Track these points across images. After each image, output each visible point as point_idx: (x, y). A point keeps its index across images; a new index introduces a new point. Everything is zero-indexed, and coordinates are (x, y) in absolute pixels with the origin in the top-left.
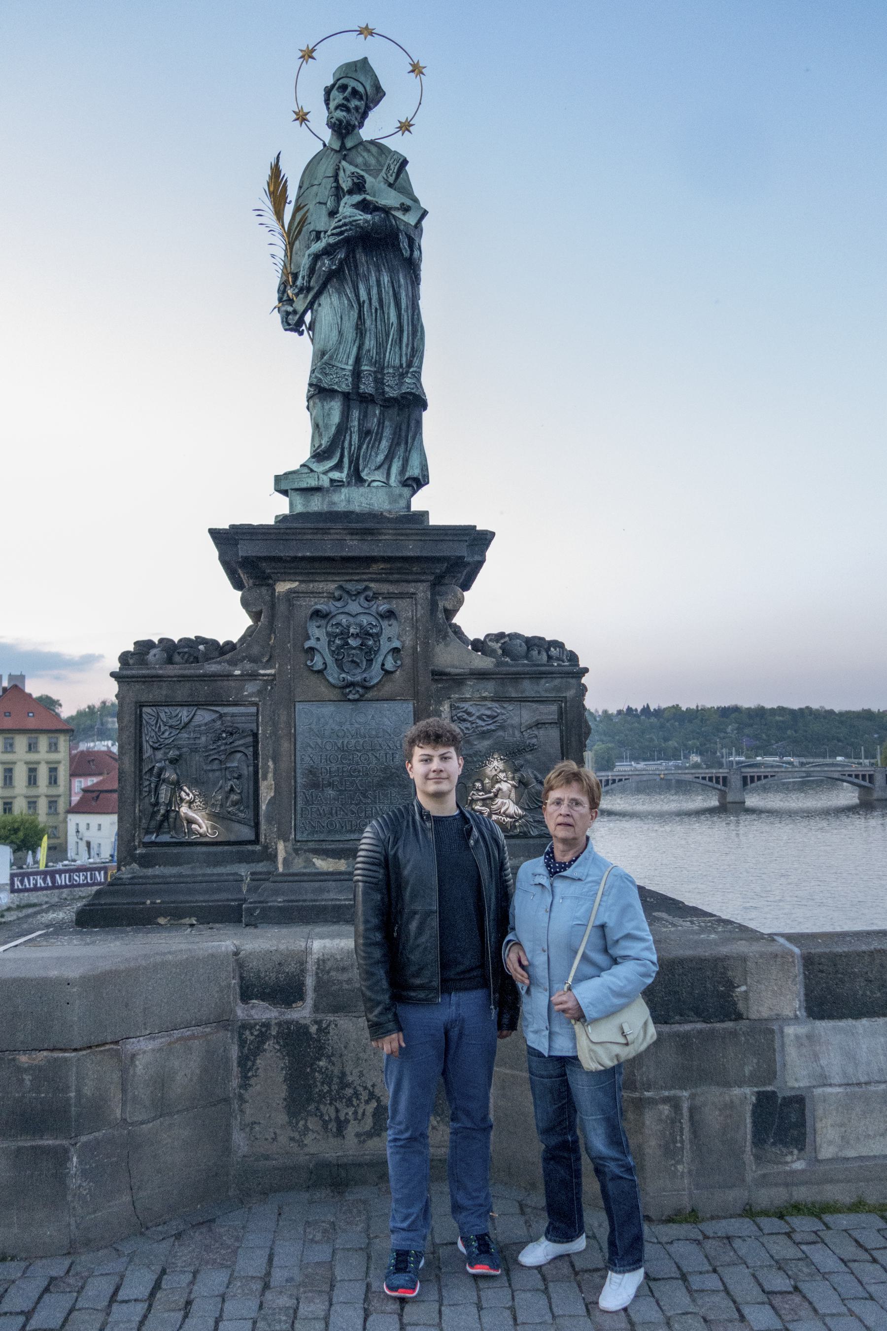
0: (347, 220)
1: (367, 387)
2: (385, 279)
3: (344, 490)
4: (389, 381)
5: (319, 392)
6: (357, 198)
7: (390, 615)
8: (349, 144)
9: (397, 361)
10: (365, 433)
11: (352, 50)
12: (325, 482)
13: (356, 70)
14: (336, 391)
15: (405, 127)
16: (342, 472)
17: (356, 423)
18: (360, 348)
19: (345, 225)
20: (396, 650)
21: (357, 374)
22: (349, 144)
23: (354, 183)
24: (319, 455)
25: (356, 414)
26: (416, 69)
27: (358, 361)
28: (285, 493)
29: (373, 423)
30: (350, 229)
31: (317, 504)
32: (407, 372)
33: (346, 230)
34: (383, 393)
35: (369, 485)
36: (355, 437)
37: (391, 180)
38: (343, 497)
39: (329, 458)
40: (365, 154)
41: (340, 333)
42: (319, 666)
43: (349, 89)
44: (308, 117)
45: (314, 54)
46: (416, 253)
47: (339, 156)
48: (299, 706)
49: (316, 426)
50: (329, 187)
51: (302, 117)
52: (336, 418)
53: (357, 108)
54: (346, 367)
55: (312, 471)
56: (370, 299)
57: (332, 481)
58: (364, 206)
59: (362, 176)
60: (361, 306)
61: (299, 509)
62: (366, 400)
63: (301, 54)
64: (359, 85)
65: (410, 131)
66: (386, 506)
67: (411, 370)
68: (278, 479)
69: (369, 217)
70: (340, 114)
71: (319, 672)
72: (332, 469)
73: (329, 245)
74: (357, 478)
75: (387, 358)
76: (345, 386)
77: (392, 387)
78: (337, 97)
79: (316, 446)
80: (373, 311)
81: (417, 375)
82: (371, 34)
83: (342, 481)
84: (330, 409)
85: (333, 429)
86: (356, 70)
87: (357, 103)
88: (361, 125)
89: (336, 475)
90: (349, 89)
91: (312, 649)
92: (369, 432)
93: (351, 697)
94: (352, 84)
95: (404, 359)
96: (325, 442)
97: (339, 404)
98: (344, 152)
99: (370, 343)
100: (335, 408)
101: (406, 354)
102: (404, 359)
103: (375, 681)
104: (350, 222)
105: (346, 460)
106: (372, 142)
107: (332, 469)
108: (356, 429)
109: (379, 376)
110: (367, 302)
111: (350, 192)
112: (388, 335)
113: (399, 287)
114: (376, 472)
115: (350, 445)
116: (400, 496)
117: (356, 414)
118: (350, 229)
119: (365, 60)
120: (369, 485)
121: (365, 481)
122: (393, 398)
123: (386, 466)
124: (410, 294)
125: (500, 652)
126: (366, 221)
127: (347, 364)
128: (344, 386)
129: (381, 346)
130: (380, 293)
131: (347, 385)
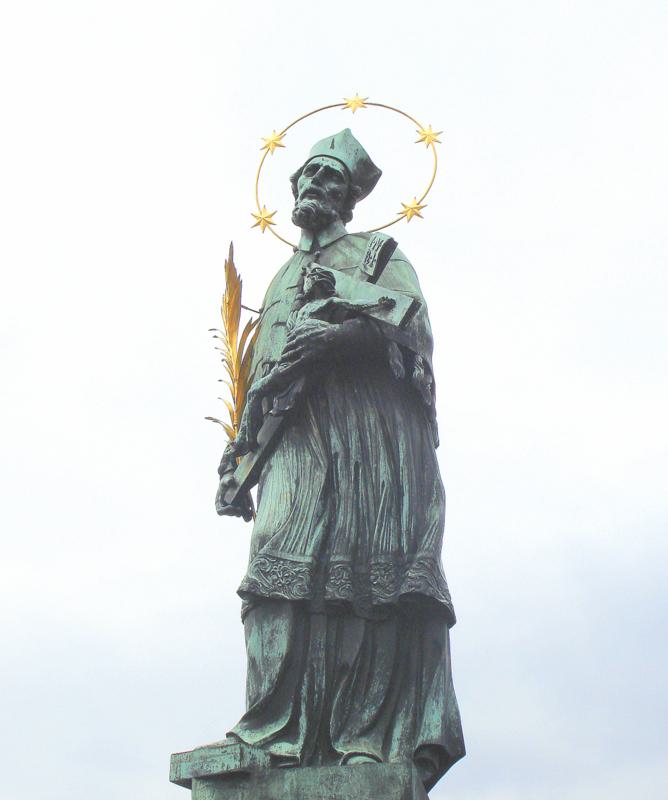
0: (302, 336)
1: (337, 589)
2: (372, 418)
3: (291, 776)
4: (378, 577)
5: (257, 603)
6: (323, 303)
8: (323, 242)
9: (393, 541)
10: (336, 671)
11: (330, 126)
12: (262, 758)
13: (332, 147)
14: (283, 600)
15: (414, 212)
16: (294, 741)
17: (322, 654)
18: (328, 529)
19: (300, 342)
21: (320, 568)
22: (323, 242)
23: (316, 284)
24: (257, 716)
25: (320, 638)
26: (428, 139)
27: (324, 545)
28: (186, 783)
29: (350, 654)
30: (308, 348)
32: (411, 562)
33: (302, 350)
34: (371, 596)
35: (344, 763)
37: (371, 272)
38: (287, 787)
40: (347, 251)
41: (294, 506)
43: (322, 168)
44: (273, 219)
45: (282, 142)
46: (419, 372)
47: (310, 258)
49: (252, 663)
50: (291, 300)
51: (265, 223)
52: (282, 645)
53: (333, 193)
54: (302, 559)
55: (240, 741)
56: (347, 451)
57: (276, 759)
58: (330, 313)
59: (328, 273)
60: (332, 460)
62: (340, 612)
63: (263, 144)
64: (336, 162)
65: (419, 215)
67: (419, 555)
69: (337, 326)
70: (307, 202)
72: (278, 737)
73: (278, 376)
74: (320, 751)
75: (375, 539)
76: (296, 593)
77: (384, 588)
78: (306, 182)
79: (253, 697)
80: (352, 468)
81: (433, 567)
82: (365, 104)
83: (293, 759)
84: (272, 631)
85: (279, 665)
86: (332, 147)
87: (333, 185)
88: (346, 216)
89: (283, 749)
90: (322, 168)
92: (344, 668)
95: (404, 540)
96: (265, 687)
97: (287, 622)
98: (315, 252)
100: (282, 627)
101: (408, 530)
102: (404, 540)
104: (307, 338)
105: (303, 721)
106: (356, 235)
107: (278, 737)
108: (322, 663)
109: (363, 570)
110: (341, 455)
111: (309, 297)
112: (377, 504)
113: (395, 426)
114: (363, 740)
115: (311, 691)
116: (392, 778)
117: (320, 638)
118: (308, 348)
119: (347, 133)
120: (344, 763)
121: (340, 755)
122: (388, 606)
123: (382, 727)
124: (417, 436)
126: (332, 334)
127: (303, 554)
128: (295, 591)
129: (362, 522)
130: (362, 440)
131: (301, 588)
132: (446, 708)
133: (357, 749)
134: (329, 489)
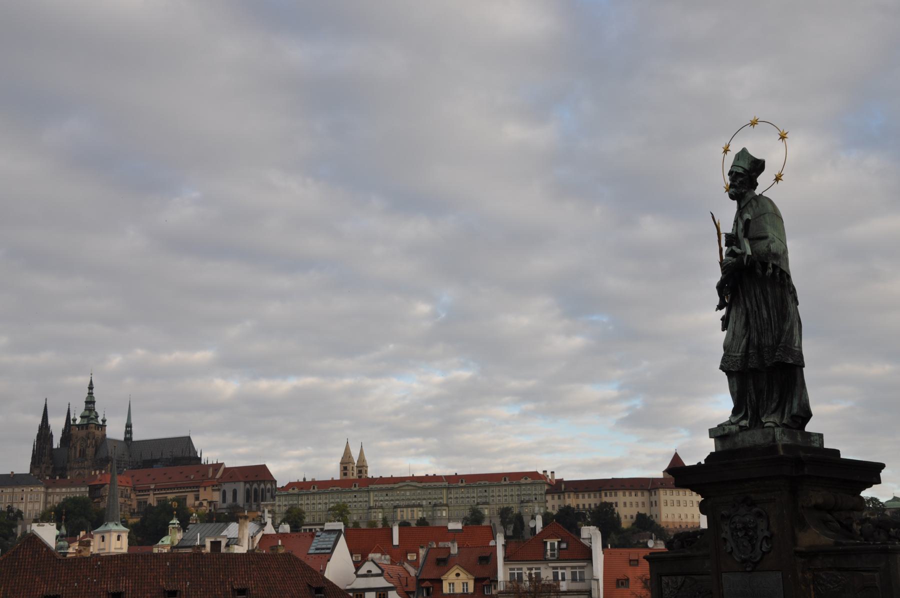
1: (753, 363)
2: (758, 291)
7: (759, 515)
8: (743, 205)
20: (766, 537)
21: (746, 355)
22: (743, 205)
24: (735, 412)
26: (783, 137)
31: (728, 445)
36: (754, 397)
39: (740, 413)
42: (729, 550)
48: (724, 575)
57: (741, 427)
61: (720, 449)
66: (762, 442)
68: (711, 431)
71: (731, 553)
72: (742, 419)
74: (756, 422)
87: (741, 179)
89: (744, 423)
91: (725, 540)
93: (748, 569)
94: (735, 170)
99: (754, 335)
103: (758, 559)
116: (769, 433)
125: (859, 533)
132: (800, 399)
133: (769, 420)
134: (747, 324)
